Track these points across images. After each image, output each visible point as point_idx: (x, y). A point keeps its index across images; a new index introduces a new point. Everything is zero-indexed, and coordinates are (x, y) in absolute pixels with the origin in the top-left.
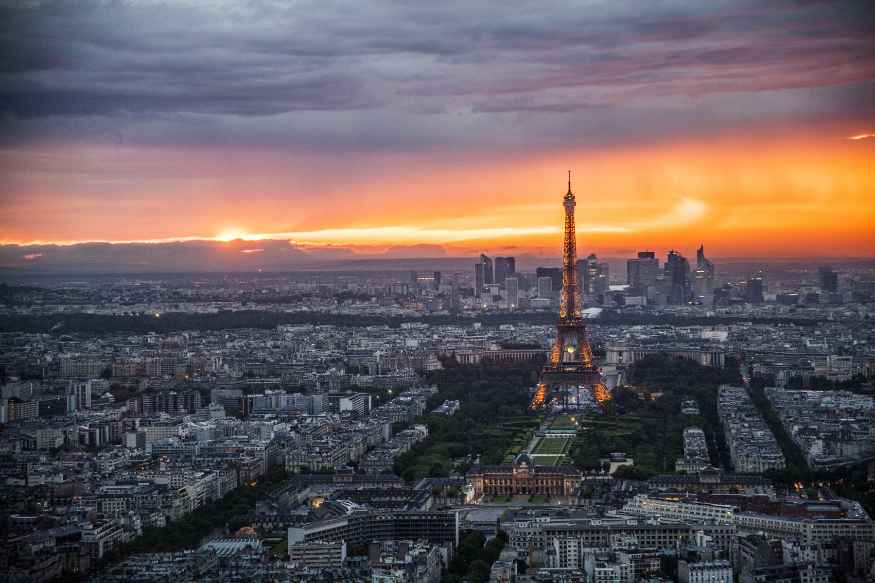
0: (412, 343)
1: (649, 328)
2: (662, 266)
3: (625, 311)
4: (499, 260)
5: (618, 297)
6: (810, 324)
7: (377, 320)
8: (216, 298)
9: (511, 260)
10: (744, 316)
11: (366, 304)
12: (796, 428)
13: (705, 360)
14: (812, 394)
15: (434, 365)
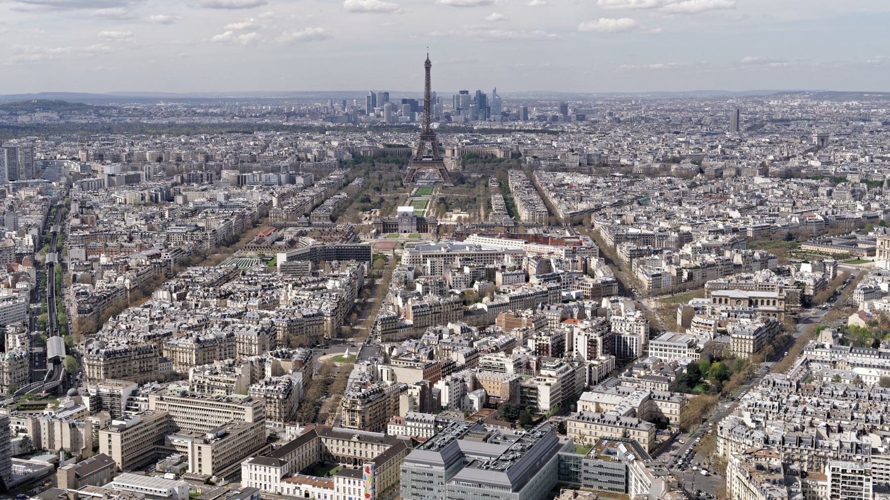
0: (335, 144)
1: (468, 134)
2: (472, 98)
3: (453, 125)
4: (380, 93)
5: (448, 117)
6: (556, 133)
7: (310, 129)
8: (216, 115)
9: (387, 94)
10: (518, 128)
11: (303, 118)
12: (553, 194)
13: (499, 154)
14: (560, 175)
15: (347, 156)
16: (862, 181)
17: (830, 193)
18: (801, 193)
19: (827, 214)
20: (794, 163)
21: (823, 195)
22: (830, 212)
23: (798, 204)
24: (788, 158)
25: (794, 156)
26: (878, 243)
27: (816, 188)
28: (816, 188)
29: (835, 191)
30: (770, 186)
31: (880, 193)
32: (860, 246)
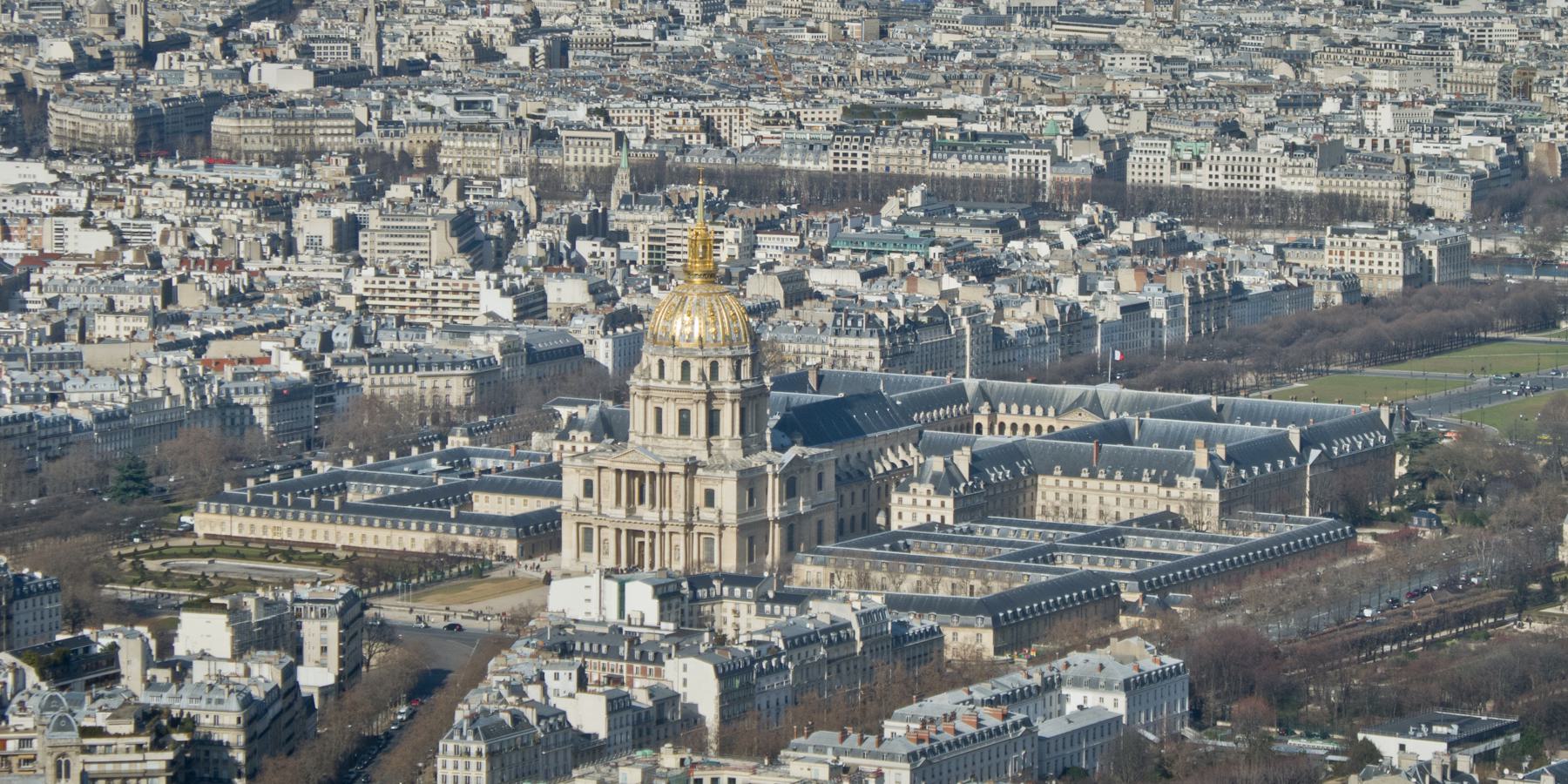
16: (513, 173)
17: (348, 234)
18: (205, 234)
19: (327, 343)
20: (183, 76)
21: (314, 244)
22: (343, 336)
23: (189, 298)
24: (146, 55)
25: (178, 42)
26: (572, 484)
27: (278, 208)
28: (278, 208)
29: (374, 220)
30: (48, 204)
31: (598, 227)
32: (484, 504)
